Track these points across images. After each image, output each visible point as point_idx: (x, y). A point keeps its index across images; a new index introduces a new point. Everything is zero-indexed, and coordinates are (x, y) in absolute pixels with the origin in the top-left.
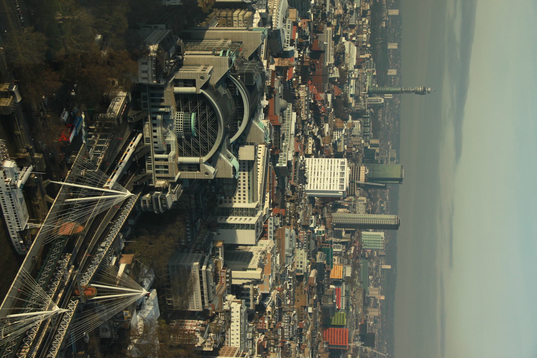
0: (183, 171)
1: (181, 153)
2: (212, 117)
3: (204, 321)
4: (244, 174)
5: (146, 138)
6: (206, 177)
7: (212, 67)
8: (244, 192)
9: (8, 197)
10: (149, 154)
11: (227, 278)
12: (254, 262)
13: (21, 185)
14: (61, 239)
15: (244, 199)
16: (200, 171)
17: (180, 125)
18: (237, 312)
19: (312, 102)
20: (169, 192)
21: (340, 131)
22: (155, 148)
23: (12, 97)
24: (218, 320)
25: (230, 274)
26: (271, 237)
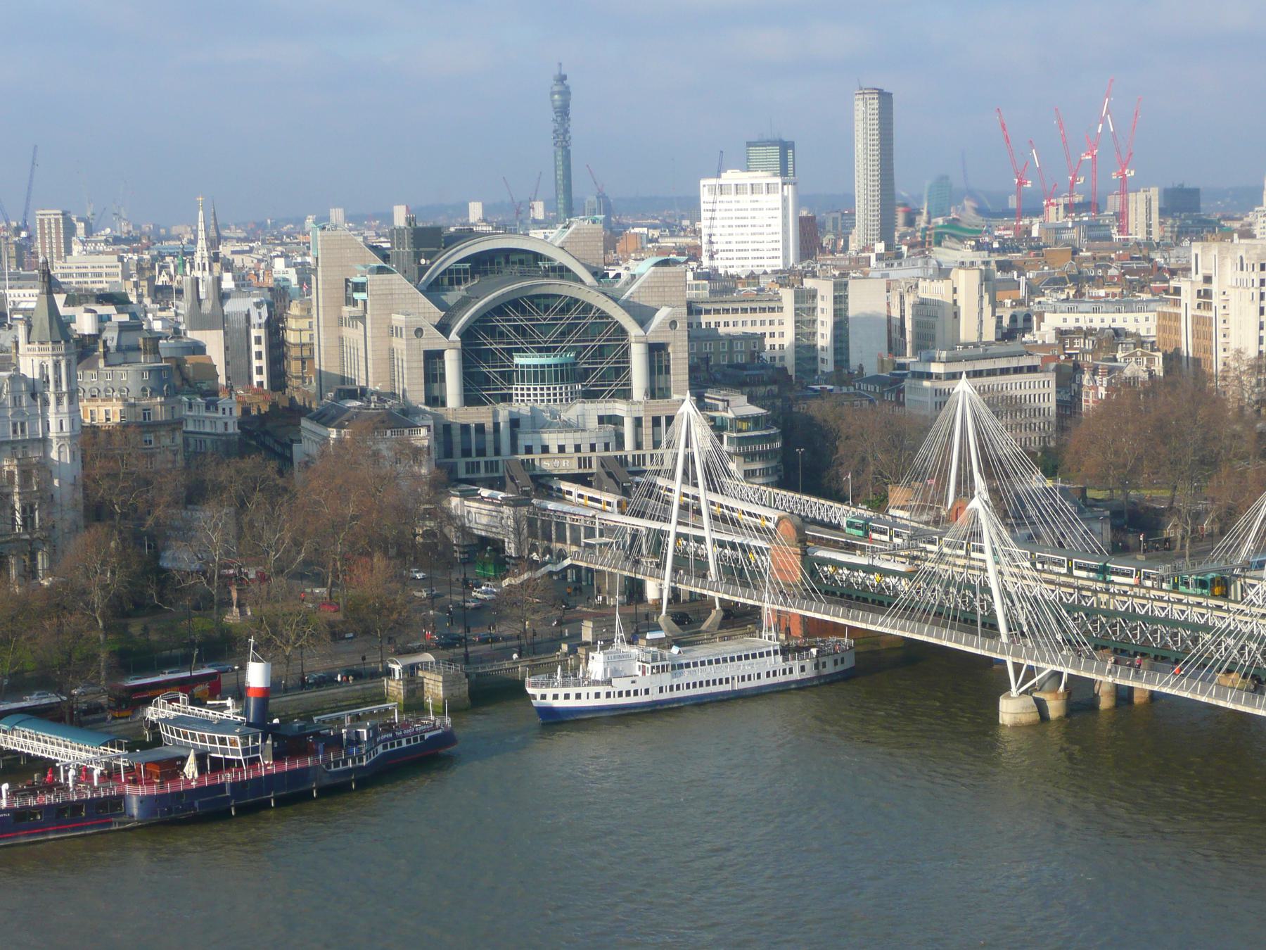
0: (668, 389)
1: (626, 394)
2: (524, 311)
5: (580, 467)
10: (622, 461)
17: (545, 392)
23: (421, 674)
24: (1084, 352)
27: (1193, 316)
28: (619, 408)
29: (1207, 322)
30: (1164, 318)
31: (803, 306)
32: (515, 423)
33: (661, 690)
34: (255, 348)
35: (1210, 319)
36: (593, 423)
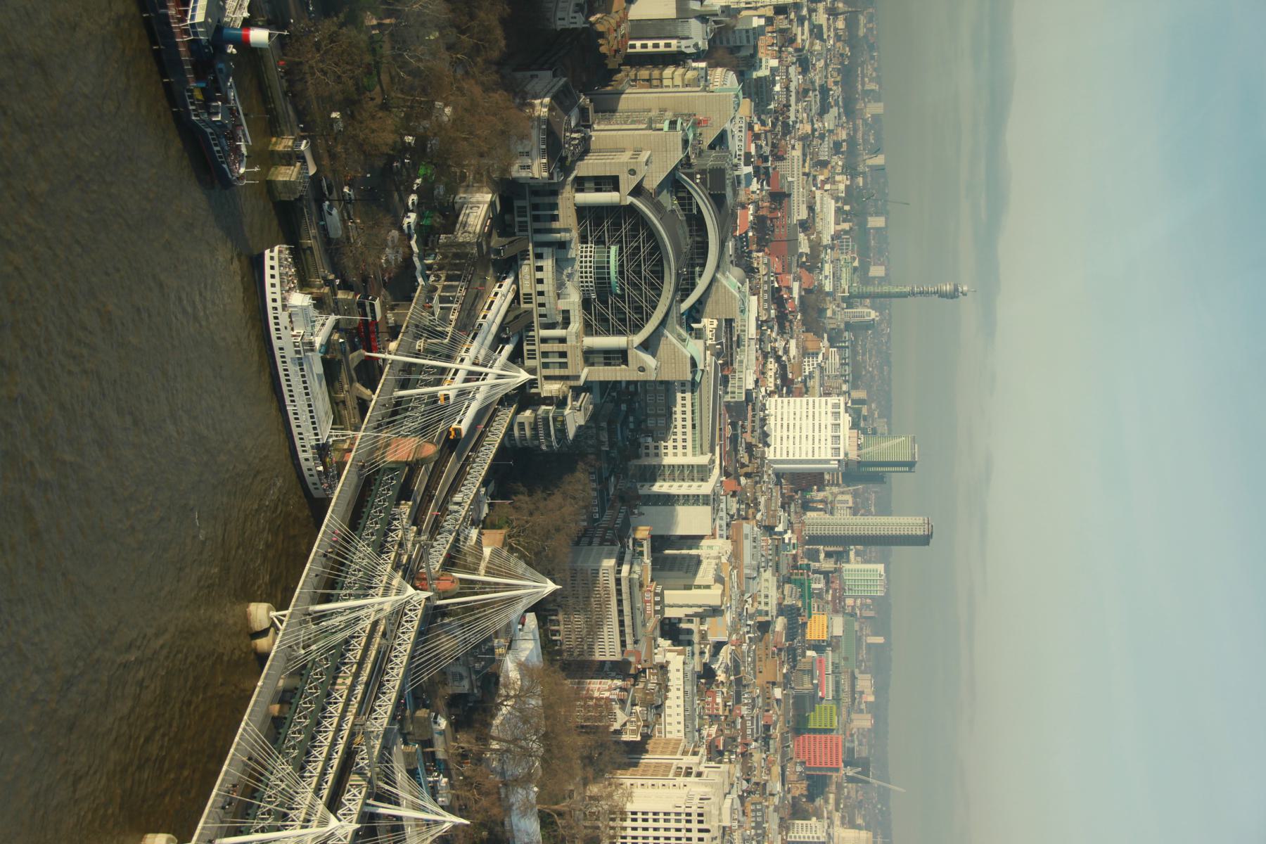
0: (592, 364)
1: (588, 329)
2: (651, 254)
3: (624, 680)
4: (684, 399)
5: (524, 294)
6: (640, 376)
7: (649, 153)
8: (684, 433)
9: (298, 368)
10: (530, 327)
11: (656, 603)
12: (706, 573)
13: (321, 345)
14: (393, 470)
15: (684, 447)
16: (627, 365)
17: (588, 270)
18: (678, 670)
19: (776, 285)
20: (569, 407)
21: (813, 358)
22: (541, 316)
24: (646, 683)
25: (661, 595)
26: (721, 536)
27: (672, 764)
28: (576, 325)
29: (666, 774)
30: (675, 744)
31: (695, 471)
32: (563, 245)
33: (281, 349)
34: (662, 43)
35: (667, 775)
36: (562, 305)
